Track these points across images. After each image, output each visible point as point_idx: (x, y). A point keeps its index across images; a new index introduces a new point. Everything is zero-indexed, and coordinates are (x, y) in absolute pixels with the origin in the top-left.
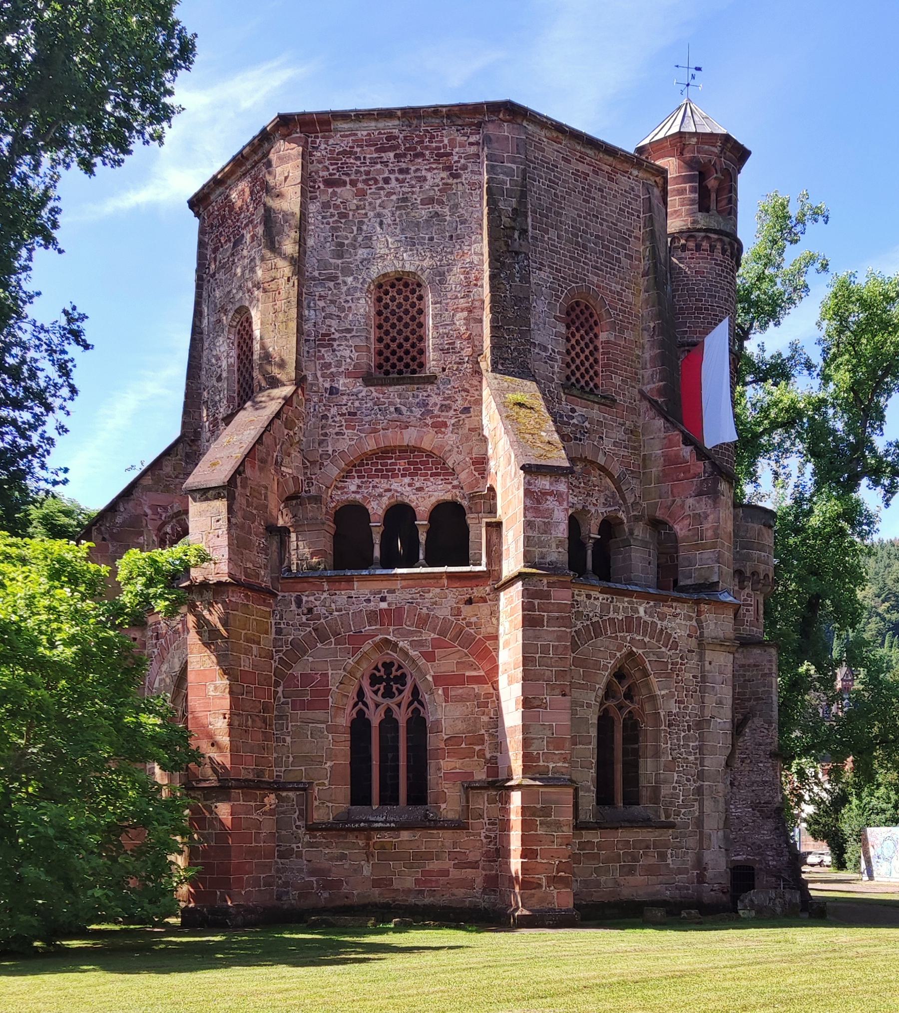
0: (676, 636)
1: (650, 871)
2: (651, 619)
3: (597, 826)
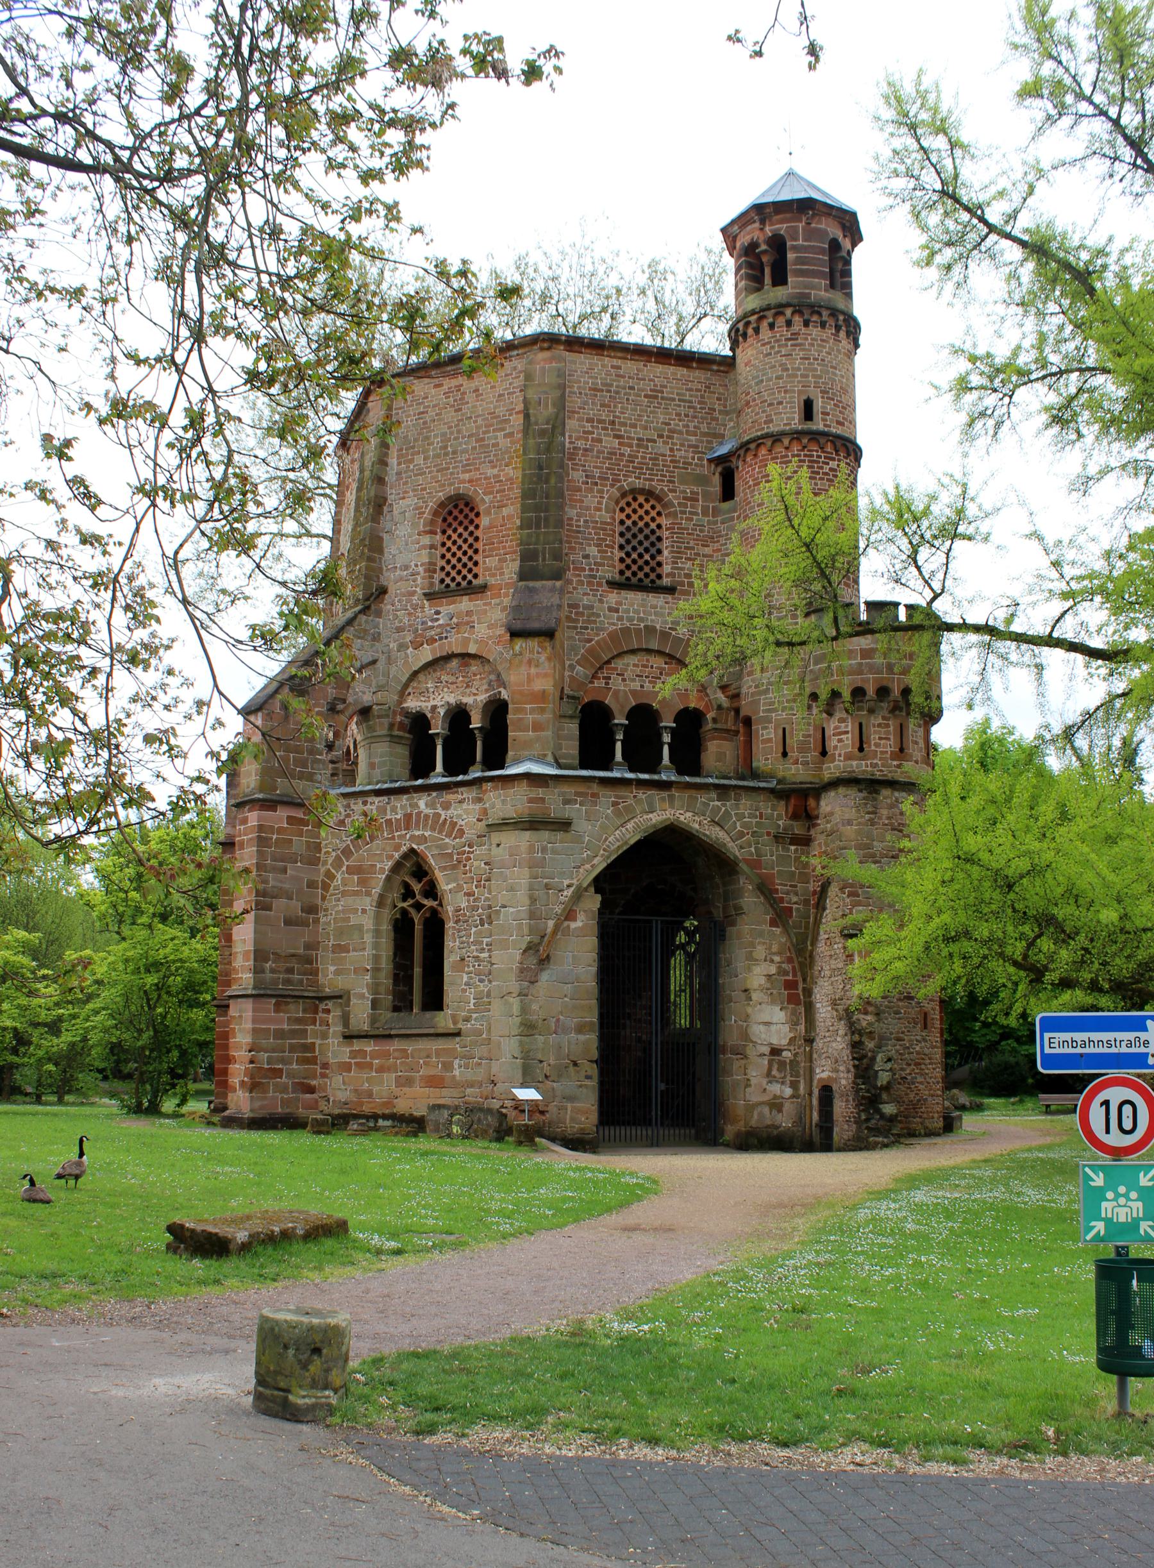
1: (434, 1082)
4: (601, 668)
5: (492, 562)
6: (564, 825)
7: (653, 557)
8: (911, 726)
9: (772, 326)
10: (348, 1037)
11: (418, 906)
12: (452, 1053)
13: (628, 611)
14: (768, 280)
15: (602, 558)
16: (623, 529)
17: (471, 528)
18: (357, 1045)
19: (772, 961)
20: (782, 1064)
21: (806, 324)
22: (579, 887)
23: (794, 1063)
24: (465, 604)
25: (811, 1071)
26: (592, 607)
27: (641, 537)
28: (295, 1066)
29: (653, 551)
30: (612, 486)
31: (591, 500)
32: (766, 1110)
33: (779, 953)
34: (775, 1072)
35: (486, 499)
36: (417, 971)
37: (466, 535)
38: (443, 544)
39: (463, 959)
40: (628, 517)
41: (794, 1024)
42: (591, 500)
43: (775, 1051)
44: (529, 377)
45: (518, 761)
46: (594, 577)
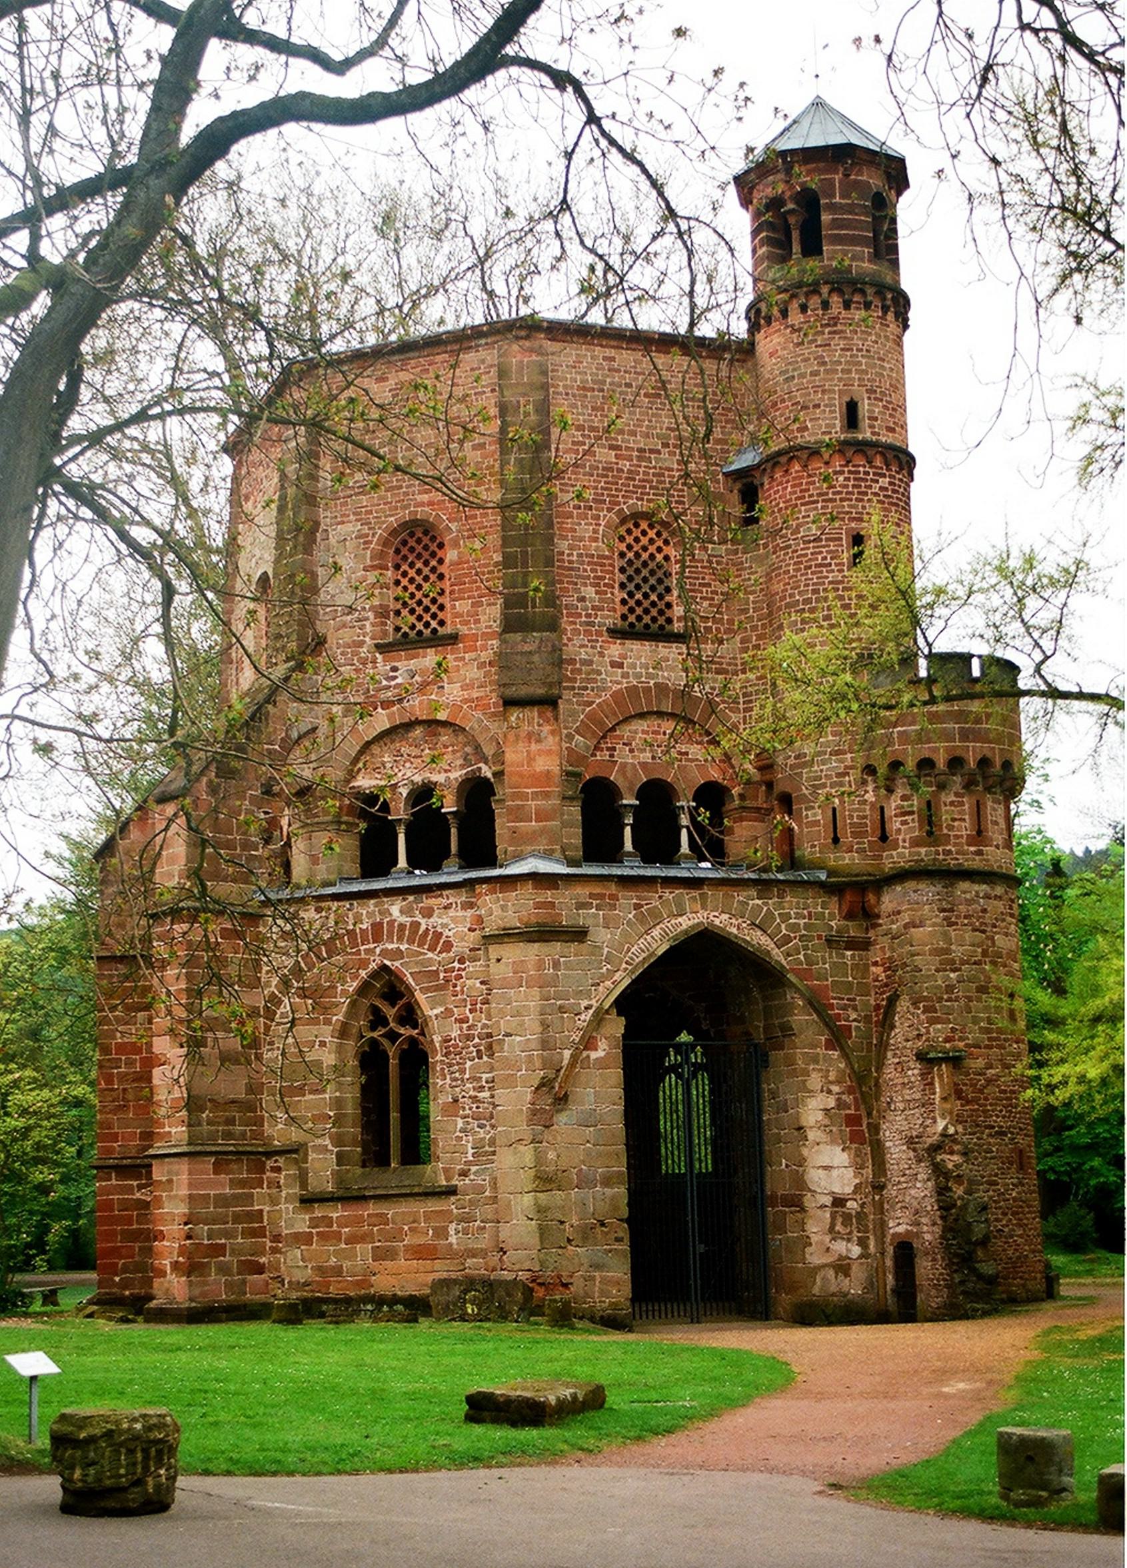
0: (450, 934)
1: (423, 1253)
2: (409, 919)
3: (347, 1197)
4: (604, 737)
5: (463, 606)
6: (579, 935)
7: (661, 597)
8: (989, 804)
9: (804, 308)
10: (308, 1201)
11: (392, 1036)
12: (445, 1215)
13: (633, 666)
14: (796, 248)
15: (601, 600)
16: (623, 563)
17: (433, 563)
18: (319, 1211)
19: (829, 1092)
20: (847, 1219)
21: (847, 305)
22: (599, 1009)
23: (861, 1216)
24: (429, 658)
25: (882, 1226)
26: (590, 663)
27: (645, 572)
28: (240, 1240)
29: (660, 589)
30: (609, 510)
31: (585, 529)
32: (831, 1273)
33: (838, 1082)
34: (838, 1228)
35: (453, 526)
36: (394, 1115)
37: (426, 571)
38: (397, 583)
39: (456, 1101)
40: (629, 547)
41: (859, 1167)
42: (585, 529)
43: (839, 1202)
44: (503, 373)
45: (519, 857)
46: (592, 624)
